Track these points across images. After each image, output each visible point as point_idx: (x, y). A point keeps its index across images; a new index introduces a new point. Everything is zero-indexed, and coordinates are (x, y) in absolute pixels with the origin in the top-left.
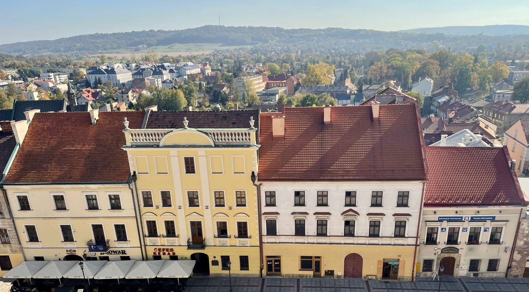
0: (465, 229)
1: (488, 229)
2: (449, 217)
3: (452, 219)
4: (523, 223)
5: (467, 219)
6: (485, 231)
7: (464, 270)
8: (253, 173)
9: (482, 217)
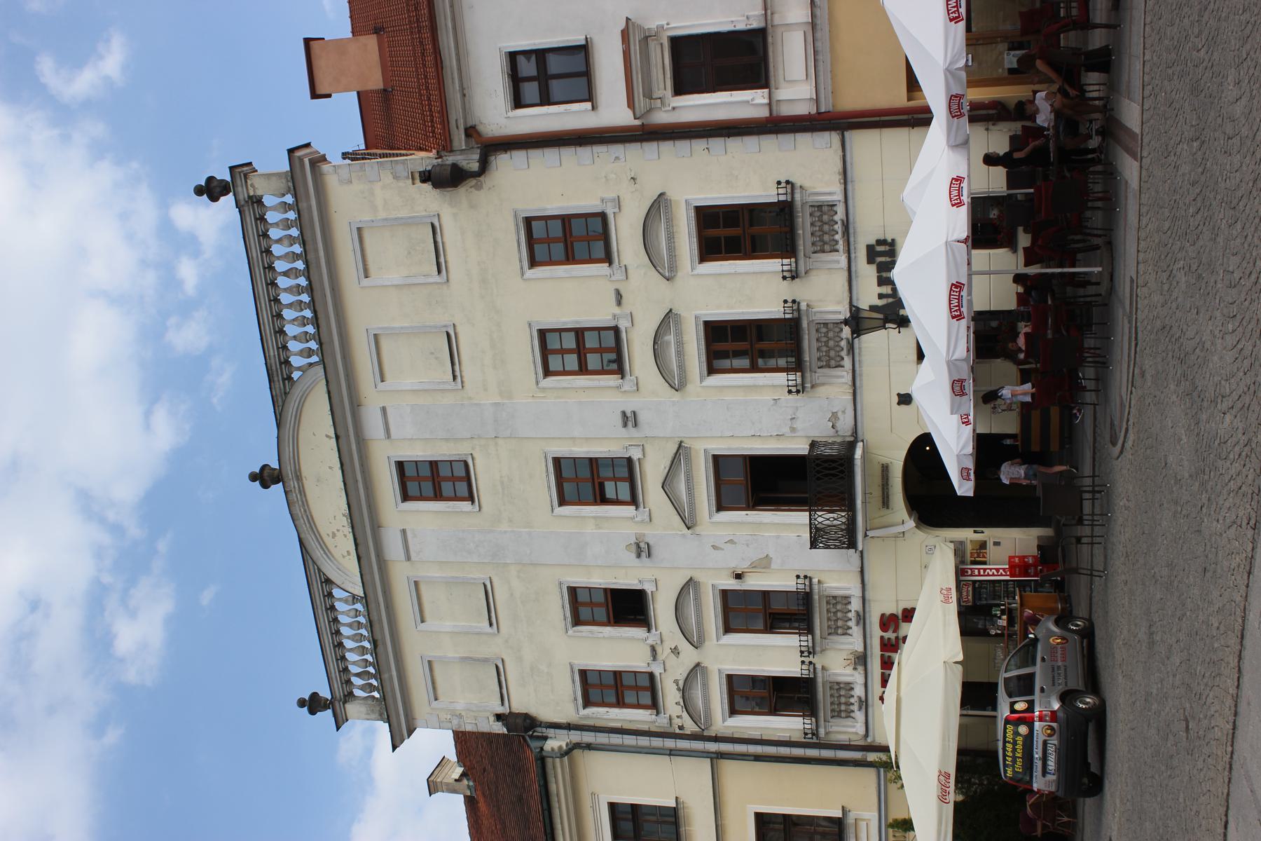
8: (426, 177)
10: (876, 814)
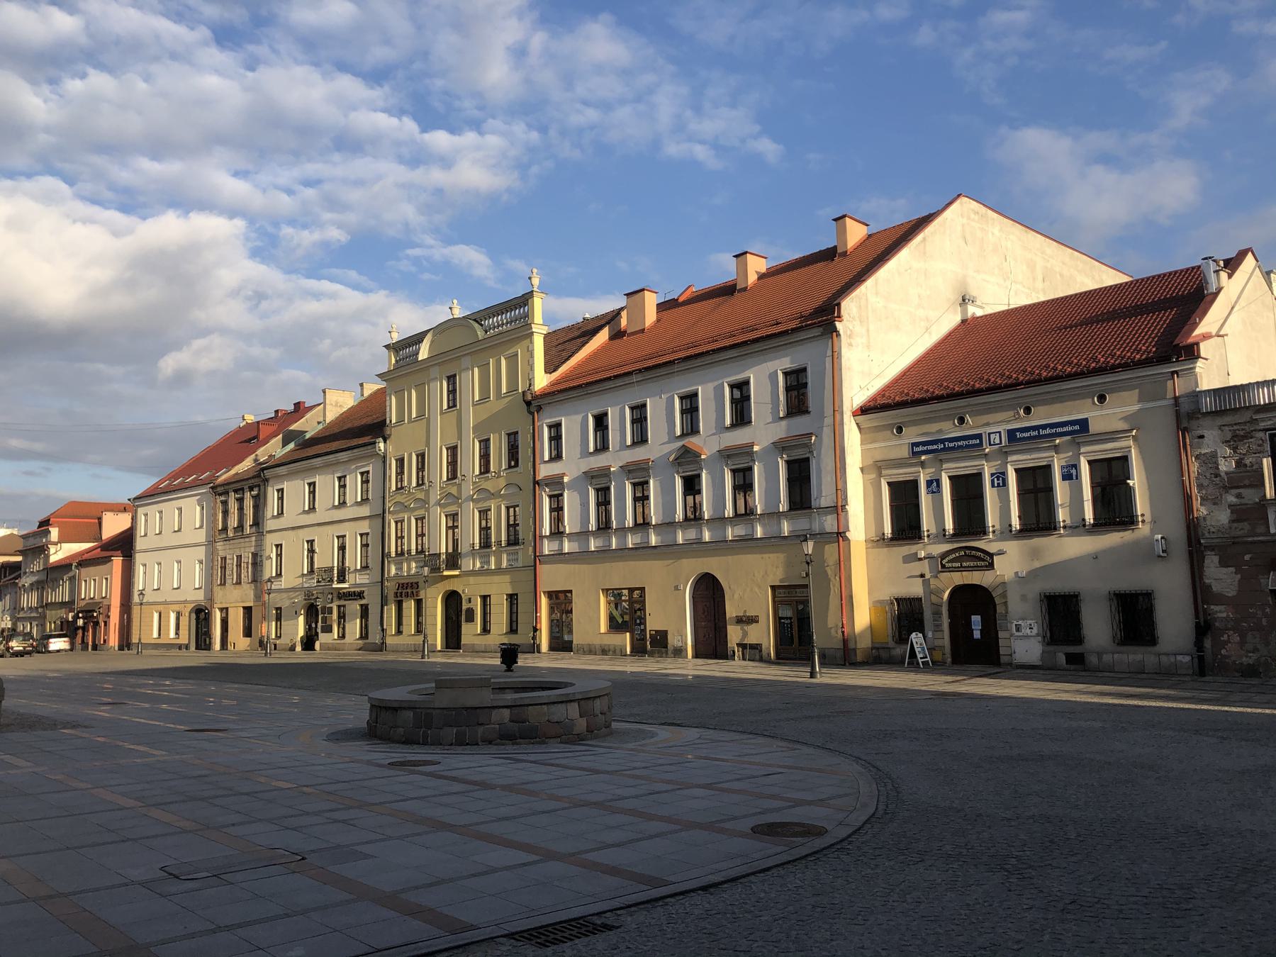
1: (1074, 471)
3: (951, 445)
4: (1200, 432)
5: (997, 441)
7: (1027, 637)
9: (1044, 427)
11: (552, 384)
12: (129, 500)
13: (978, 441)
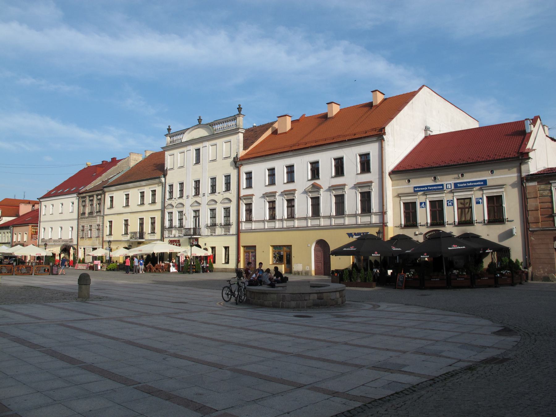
0: (450, 205)
1: (481, 201)
2: (427, 186)
3: (431, 188)
6: (478, 203)
9: (469, 182)
10: (156, 239)
11: (246, 154)
12: (38, 199)
13: (442, 187)
